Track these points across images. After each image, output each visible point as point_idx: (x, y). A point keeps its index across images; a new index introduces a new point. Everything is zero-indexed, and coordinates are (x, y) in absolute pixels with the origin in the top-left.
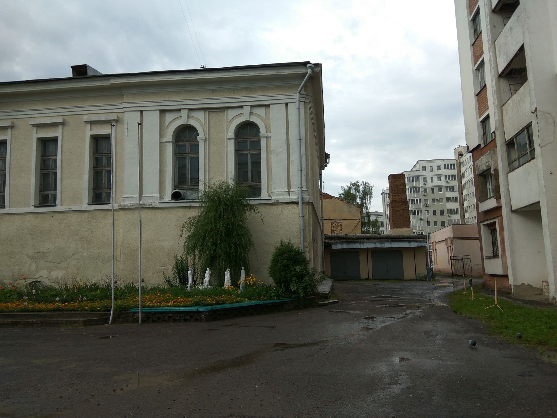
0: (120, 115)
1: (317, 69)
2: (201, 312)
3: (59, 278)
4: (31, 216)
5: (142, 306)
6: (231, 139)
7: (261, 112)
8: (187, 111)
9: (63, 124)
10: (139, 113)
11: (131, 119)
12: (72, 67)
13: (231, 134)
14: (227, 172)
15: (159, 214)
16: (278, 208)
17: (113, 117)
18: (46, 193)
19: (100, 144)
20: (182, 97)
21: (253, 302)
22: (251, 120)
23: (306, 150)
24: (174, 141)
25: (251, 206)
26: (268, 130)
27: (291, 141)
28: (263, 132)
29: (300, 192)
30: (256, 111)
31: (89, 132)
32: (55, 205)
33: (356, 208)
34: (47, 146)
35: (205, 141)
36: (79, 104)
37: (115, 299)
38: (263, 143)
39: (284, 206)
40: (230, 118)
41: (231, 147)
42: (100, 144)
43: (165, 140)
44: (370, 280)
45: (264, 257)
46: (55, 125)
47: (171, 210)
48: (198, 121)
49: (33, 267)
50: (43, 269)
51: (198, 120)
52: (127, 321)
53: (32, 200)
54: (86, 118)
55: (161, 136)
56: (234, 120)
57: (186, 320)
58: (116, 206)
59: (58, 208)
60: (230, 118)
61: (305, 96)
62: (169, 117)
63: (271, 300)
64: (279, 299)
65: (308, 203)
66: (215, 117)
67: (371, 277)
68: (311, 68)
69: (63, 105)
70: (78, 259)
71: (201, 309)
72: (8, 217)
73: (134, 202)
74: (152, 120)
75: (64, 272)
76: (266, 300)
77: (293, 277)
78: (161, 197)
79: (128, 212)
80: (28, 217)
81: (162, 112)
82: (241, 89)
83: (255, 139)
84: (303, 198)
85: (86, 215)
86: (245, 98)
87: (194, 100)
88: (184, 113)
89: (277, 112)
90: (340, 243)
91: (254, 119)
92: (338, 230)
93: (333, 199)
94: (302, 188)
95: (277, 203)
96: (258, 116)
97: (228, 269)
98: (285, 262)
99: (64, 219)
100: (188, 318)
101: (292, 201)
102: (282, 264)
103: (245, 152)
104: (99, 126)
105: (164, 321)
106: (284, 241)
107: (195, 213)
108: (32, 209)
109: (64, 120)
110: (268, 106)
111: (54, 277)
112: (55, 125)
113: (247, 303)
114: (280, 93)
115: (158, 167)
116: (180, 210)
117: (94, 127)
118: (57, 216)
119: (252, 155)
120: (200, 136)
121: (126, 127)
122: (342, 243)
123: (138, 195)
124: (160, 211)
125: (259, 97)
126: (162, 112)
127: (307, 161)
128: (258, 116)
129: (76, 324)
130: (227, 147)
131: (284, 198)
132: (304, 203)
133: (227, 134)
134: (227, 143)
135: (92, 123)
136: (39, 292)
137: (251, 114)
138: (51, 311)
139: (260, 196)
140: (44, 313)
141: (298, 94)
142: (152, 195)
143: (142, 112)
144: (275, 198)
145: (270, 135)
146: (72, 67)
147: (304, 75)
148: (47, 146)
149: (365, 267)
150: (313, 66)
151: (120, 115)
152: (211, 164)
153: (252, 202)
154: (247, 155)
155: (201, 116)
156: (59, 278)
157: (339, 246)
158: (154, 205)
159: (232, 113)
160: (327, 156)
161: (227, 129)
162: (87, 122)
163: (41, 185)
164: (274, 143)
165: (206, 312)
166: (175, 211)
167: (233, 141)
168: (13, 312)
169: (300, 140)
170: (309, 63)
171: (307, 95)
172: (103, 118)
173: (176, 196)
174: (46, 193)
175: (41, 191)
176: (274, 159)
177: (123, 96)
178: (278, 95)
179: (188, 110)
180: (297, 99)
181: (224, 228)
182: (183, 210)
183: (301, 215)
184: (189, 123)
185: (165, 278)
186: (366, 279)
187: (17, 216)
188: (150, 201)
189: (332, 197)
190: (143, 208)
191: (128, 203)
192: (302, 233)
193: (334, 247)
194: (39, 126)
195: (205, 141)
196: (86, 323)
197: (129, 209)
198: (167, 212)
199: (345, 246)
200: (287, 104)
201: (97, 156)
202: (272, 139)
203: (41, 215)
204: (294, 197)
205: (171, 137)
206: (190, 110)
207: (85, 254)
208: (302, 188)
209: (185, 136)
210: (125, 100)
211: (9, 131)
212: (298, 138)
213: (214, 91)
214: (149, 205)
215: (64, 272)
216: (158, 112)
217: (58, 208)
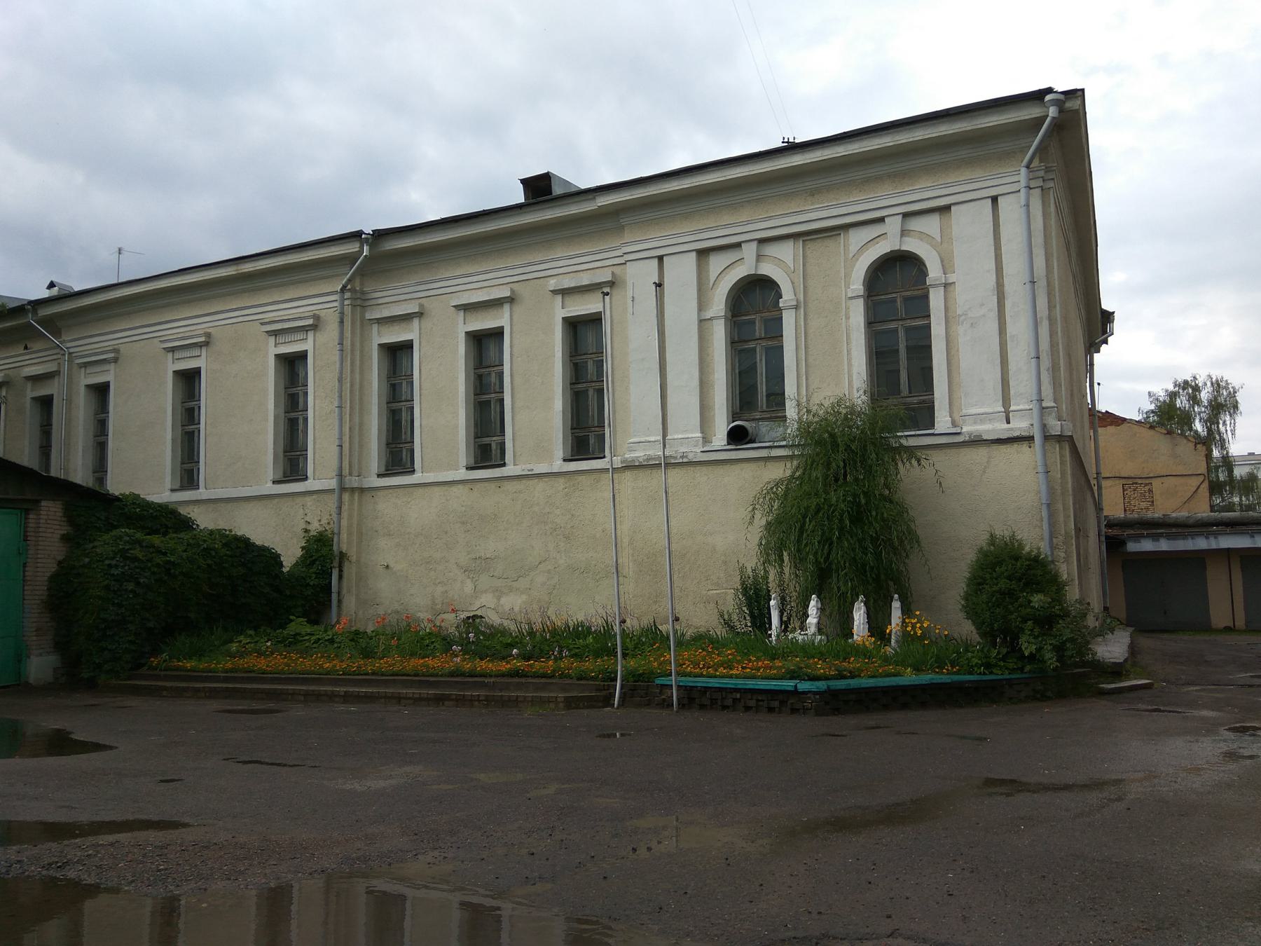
0: (617, 270)
1: (1072, 104)
2: (804, 693)
3: (517, 609)
4: (460, 486)
5: (678, 674)
6: (858, 297)
7: (931, 225)
8: (754, 245)
9: (511, 300)
10: (656, 260)
11: (640, 276)
12: (523, 181)
13: (857, 286)
14: (850, 376)
15: (701, 475)
16: (981, 453)
17: (605, 276)
18: (486, 440)
20: (744, 215)
21: (926, 678)
22: (904, 248)
23: (1051, 307)
24: (730, 315)
25: (911, 452)
26: (946, 267)
27: (1008, 288)
28: (934, 271)
29: (1036, 412)
30: (917, 224)
31: (562, 310)
32: (504, 465)
33: (1191, 445)
34: (484, 344)
35: (797, 307)
36: (539, 257)
37: (624, 655)
38: (936, 300)
39: (995, 447)
40: (853, 248)
41: (857, 315)
43: (709, 314)
44: (1240, 631)
45: (948, 570)
46: (496, 304)
47: (727, 467)
48: (781, 265)
49: (469, 587)
50: (486, 592)
51: (779, 262)
52: (648, 704)
53: (462, 453)
54: (553, 284)
55: (701, 307)
56: (863, 251)
57: (771, 710)
58: (617, 462)
59: (509, 470)
60: (853, 248)
61: (1042, 173)
62: (716, 263)
63: (970, 673)
64: (991, 673)
65: (1060, 438)
66: (818, 249)
67: (1240, 623)
68: (1055, 102)
69: (510, 262)
70: (549, 572)
71: (804, 686)
72: (421, 490)
73: (650, 452)
75: (524, 597)
76: (957, 673)
77: (1025, 621)
78: (706, 440)
79: (641, 474)
80: (456, 490)
81: (703, 254)
82: (879, 179)
83: (916, 293)
84: (1044, 427)
85: (561, 480)
86: (887, 198)
87: (770, 218)
88: (749, 251)
89: (970, 223)
90: (1148, 536)
91: (911, 245)
92: (1143, 505)
93: (1125, 426)
94: (1040, 400)
95: (977, 441)
96: (923, 236)
97: (861, 597)
98: (1003, 584)
99: (520, 492)
100: (776, 704)
101: (1016, 434)
102: (995, 588)
103: (893, 325)
105: (724, 708)
106: (998, 533)
107: (779, 472)
108: (462, 474)
109: (512, 291)
110: (946, 209)
111: (507, 608)
112: (496, 304)
113: (909, 678)
114: (978, 173)
115: (696, 374)
116: (745, 465)
117: (569, 300)
119: (908, 330)
120: (785, 297)
121: (630, 294)
122: (1155, 537)
123: (660, 438)
124: (704, 468)
125: (924, 191)
126: (703, 254)
127: (1052, 334)
128: (923, 236)
129: (552, 706)
130: (848, 318)
131: (997, 428)
132: (1047, 438)
133: (847, 286)
134: (847, 308)
135: (565, 292)
136: (480, 638)
137: (904, 233)
138: (503, 675)
139: (932, 425)
140: (492, 680)
141: (1023, 171)
142: (686, 436)
143: (661, 258)
144: (968, 429)
145: (952, 278)
146: (523, 181)
147: (1039, 121)
148: (484, 344)
149: (1224, 599)
150: (1062, 97)
151: (617, 270)
152: (810, 360)
153: (912, 442)
154: (896, 330)
155: (786, 252)
156: (517, 609)
157: (1147, 546)
158: (691, 457)
159: (857, 238)
160: (1108, 317)
161: (847, 276)
162: (555, 292)
163: (476, 425)
164: (962, 297)
165: (815, 693)
166: (736, 468)
167: (861, 302)
168: (437, 675)
169: (1033, 282)
170: (1049, 90)
171: (1048, 170)
172: (585, 280)
173: (737, 436)
174: (486, 440)
175: (476, 437)
176: (963, 336)
177: (623, 227)
178: (971, 181)
180: (1023, 183)
181: (847, 502)
182: (753, 466)
183: (1040, 469)
184: (760, 272)
185: (722, 616)
186: (1228, 630)
187: (436, 489)
188: (683, 449)
189: (1124, 420)
190: (669, 464)
191: (639, 454)
192: (1045, 514)
193: (1132, 547)
194: (467, 308)
195: (797, 307)
196: (571, 703)
197: (641, 466)
198: (720, 470)
199: (1164, 545)
200: (995, 199)
201: (578, 359)
202: (958, 288)
203: (479, 485)
204: (1020, 425)
205: (722, 306)
206: (762, 241)
207: (561, 562)
208: (1040, 400)
209: (754, 302)
210: (628, 237)
212: (1027, 278)
213: (813, 193)
214: (682, 457)
215: (524, 597)
216: (694, 254)
217: (509, 470)
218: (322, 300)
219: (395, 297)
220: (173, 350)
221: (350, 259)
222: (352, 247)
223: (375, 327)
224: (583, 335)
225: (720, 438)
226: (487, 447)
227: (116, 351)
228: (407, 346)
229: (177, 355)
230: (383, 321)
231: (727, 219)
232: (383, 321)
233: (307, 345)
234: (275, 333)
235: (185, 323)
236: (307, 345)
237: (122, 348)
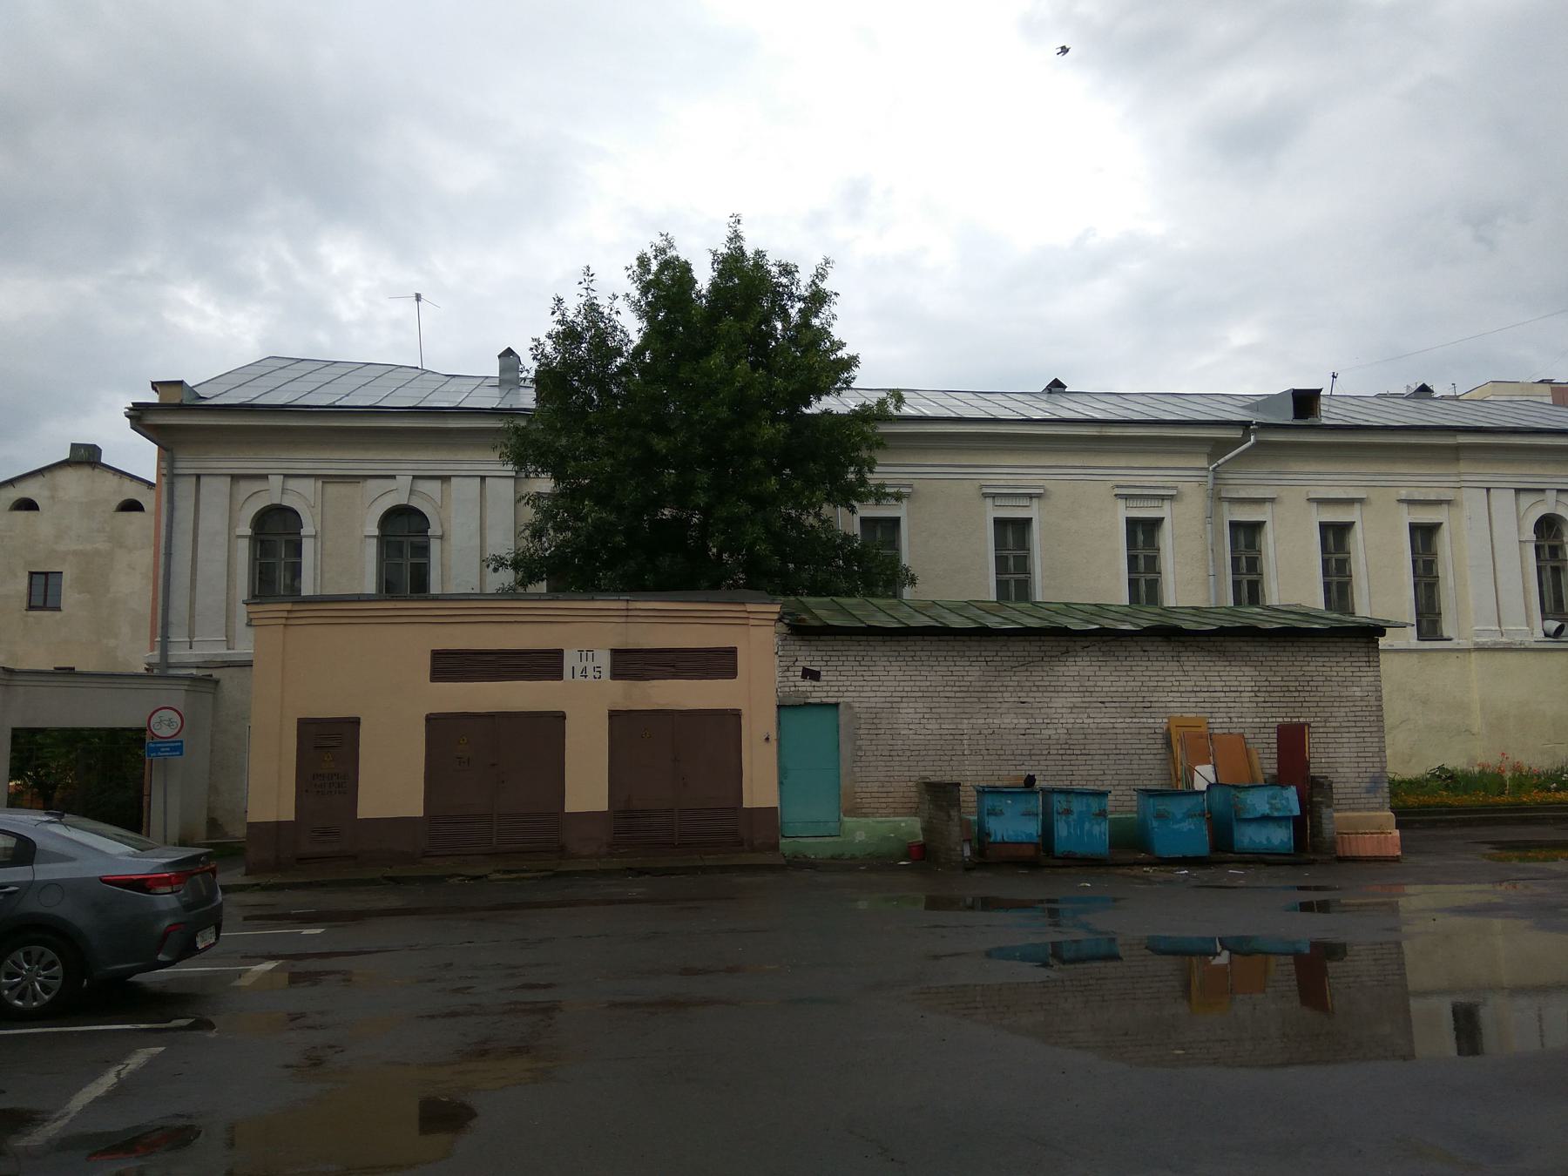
11: (1473, 500)
15: (1530, 657)
19: (1423, 535)
20: (1550, 470)
34: (1335, 536)
42: (1423, 535)
46: (1350, 502)
54: (1404, 494)
62: (1526, 500)
79: (1486, 655)
81: (1518, 491)
85: (1415, 655)
112: (1350, 502)
126: (1518, 491)
135: (1411, 502)
143: (1488, 489)
148: (1335, 536)
166: (1557, 656)
177: (1458, 460)
188: (1518, 639)
190: (1508, 649)
198: (1545, 656)
206: (1559, 491)
210: (1463, 467)
211: (1268, 506)
219: (1250, 481)
220: (994, 496)
222: (1237, 434)
223: (1226, 505)
225: (1540, 635)
227: (910, 486)
228: (1257, 527)
230: (1233, 501)
231: (1537, 470)
232: (1233, 501)
233: (1164, 511)
234: (1127, 497)
235: (1007, 471)
236: (1164, 511)
237: (916, 484)
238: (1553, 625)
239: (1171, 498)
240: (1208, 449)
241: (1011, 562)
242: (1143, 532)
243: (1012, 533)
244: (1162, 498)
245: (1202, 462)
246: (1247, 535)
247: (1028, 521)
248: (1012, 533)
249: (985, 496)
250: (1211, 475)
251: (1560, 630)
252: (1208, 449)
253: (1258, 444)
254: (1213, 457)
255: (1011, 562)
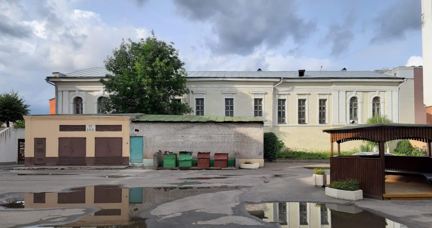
9: (309, 94)
34: (301, 102)
46: (305, 94)
74: (343, 94)
104: (322, 96)
112: (305, 94)
118: (307, 127)
135: (320, 94)
148: (301, 102)
179: (354, 90)
194: (299, 94)
218: (269, 89)
219: (282, 90)
221: (278, 82)
222: (278, 80)
224: (322, 102)
225: (349, 123)
226: (301, 120)
229: (226, 95)
234: (255, 94)
238: (351, 121)
239: (265, 94)
240: (273, 83)
241: (229, 108)
242: (258, 101)
243: (229, 102)
244: (262, 94)
245: (272, 86)
246: (281, 102)
247: (233, 99)
248: (229, 102)
249: (223, 94)
250: (273, 89)
251: (353, 122)
252: (273, 83)
253: (283, 82)
254: (274, 85)
255: (229, 108)
